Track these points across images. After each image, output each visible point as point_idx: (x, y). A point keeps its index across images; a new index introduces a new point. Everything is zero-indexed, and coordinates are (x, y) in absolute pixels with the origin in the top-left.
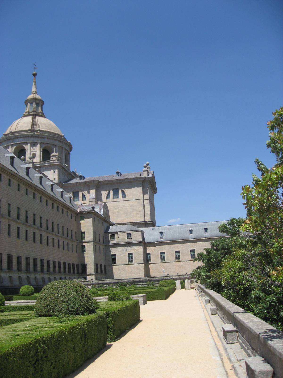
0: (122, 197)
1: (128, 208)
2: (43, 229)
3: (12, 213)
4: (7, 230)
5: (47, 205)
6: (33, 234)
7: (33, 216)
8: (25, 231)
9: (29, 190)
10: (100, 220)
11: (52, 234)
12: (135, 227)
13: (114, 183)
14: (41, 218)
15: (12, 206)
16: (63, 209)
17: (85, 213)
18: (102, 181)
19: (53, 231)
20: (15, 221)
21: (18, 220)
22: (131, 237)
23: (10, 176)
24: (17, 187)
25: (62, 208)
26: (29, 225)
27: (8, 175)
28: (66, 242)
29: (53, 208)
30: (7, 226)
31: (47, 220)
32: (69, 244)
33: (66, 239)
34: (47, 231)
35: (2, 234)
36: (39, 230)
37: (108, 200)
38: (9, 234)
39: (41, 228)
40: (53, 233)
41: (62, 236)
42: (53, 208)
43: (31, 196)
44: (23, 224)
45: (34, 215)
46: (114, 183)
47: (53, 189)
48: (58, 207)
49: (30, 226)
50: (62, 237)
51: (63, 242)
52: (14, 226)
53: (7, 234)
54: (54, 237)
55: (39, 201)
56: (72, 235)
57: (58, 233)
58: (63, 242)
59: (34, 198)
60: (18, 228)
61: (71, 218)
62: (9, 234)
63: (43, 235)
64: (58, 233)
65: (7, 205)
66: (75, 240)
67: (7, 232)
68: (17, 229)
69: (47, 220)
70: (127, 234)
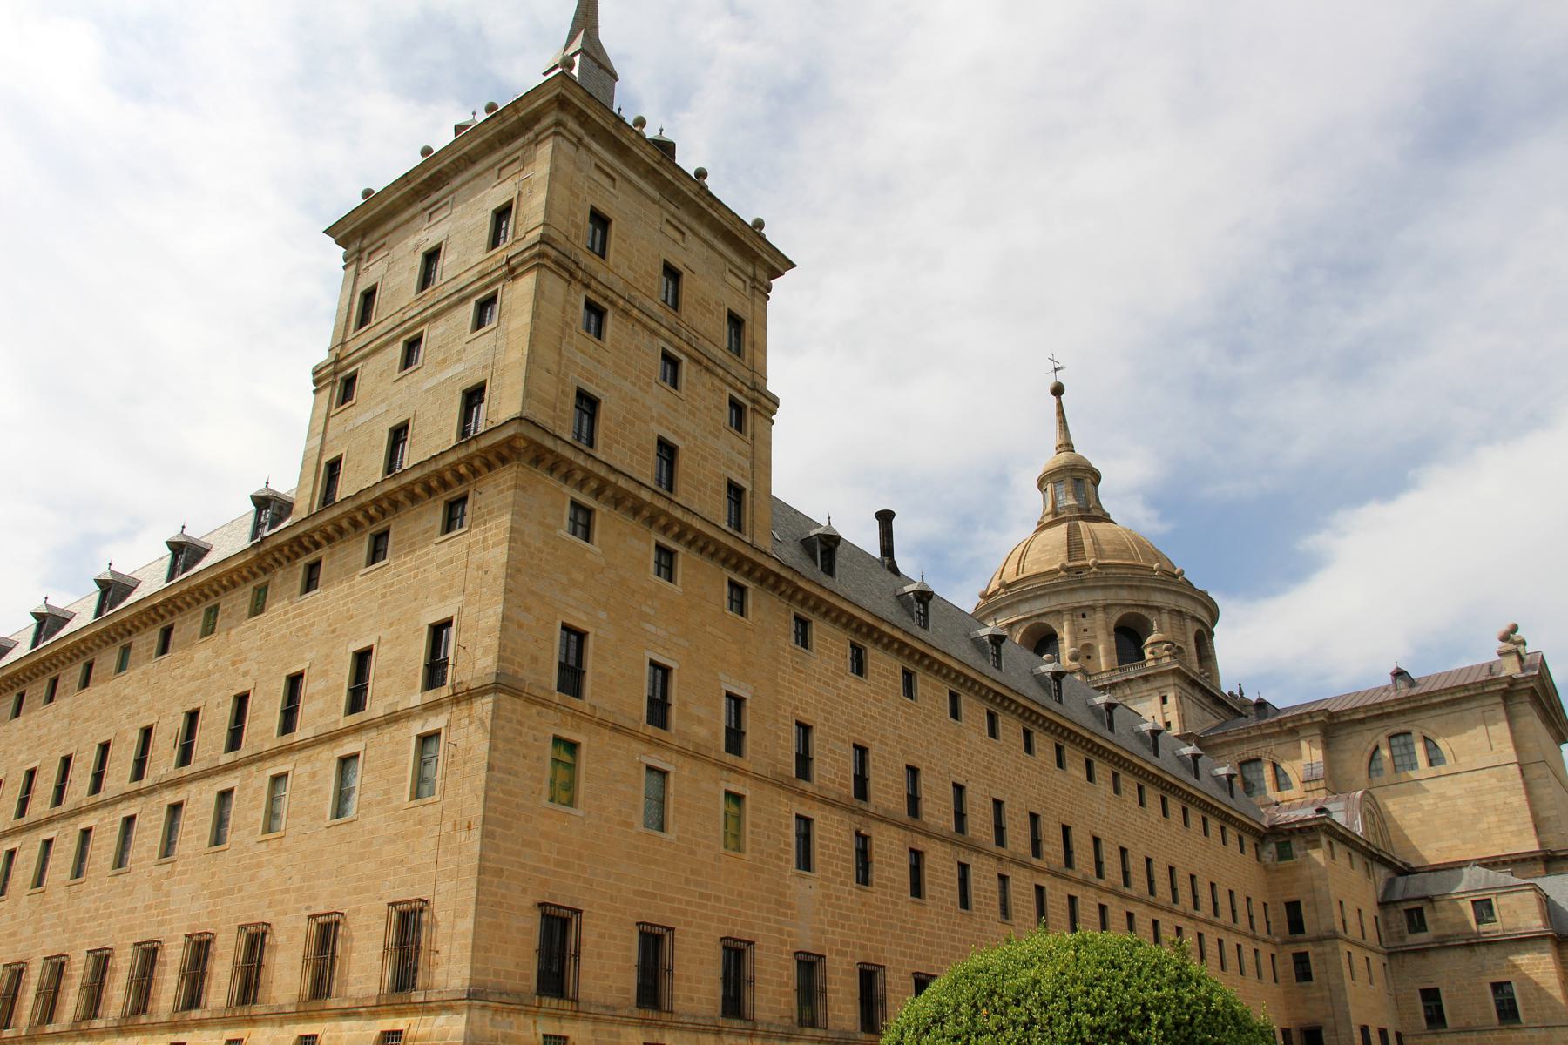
0: (1431, 763)
1: (1460, 802)
2: (1134, 894)
3: (1009, 833)
4: (997, 896)
5: (1142, 803)
6: (1097, 910)
7: (1091, 844)
8: (1066, 902)
9: (1069, 751)
10: (1354, 854)
11: (1171, 911)
12: (1503, 877)
13: (1389, 715)
14: (1123, 851)
15: (1006, 807)
16: (1204, 819)
17: (1291, 831)
18: (1342, 712)
19: (1175, 900)
20: (1024, 865)
21: (1034, 861)
22: (1492, 914)
23: (992, 701)
24: (1021, 742)
25: (1200, 814)
26: (1079, 876)
27: (984, 697)
28: (1231, 941)
29: (1165, 814)
30: (996, 883)
31: (1148, 860)
32: (1243, 949)
33: (1228, 929)
34: (1152, 899)
35: (978, 910)
36: (1122, 896)
37: (1377, 780)
38: (1005, 911)
39: (1127, 891)
40: (1176, 907)
41: (1212, 918)
42: (1165, 814)
43: (1076, 770)
44: (1056, 875)
45: (1097, 840)
46: (1389, 715)
47: (1161, 750)
48: (1185, 810)
49: (1085, 883)
50: (1211, 924)
51: (1220, 941)
52: (1022, 884)
53: (997, 909)
54: (1182, 922)
55: (1110, 788)
56: (1251, 917)
57: (1196, 907)
58: (1220, 941)
59: (1090, 778)
60: (1040, 890)
61: (1242, 851)
62: (1005, 911)
63: (1136, 916)
64: (1196, 907)
65: (990, 805)
66: (1266, 936)
67: (997, 903)
68: (1033, 892)
69: (1148, 860)
70: (1474, 902)
